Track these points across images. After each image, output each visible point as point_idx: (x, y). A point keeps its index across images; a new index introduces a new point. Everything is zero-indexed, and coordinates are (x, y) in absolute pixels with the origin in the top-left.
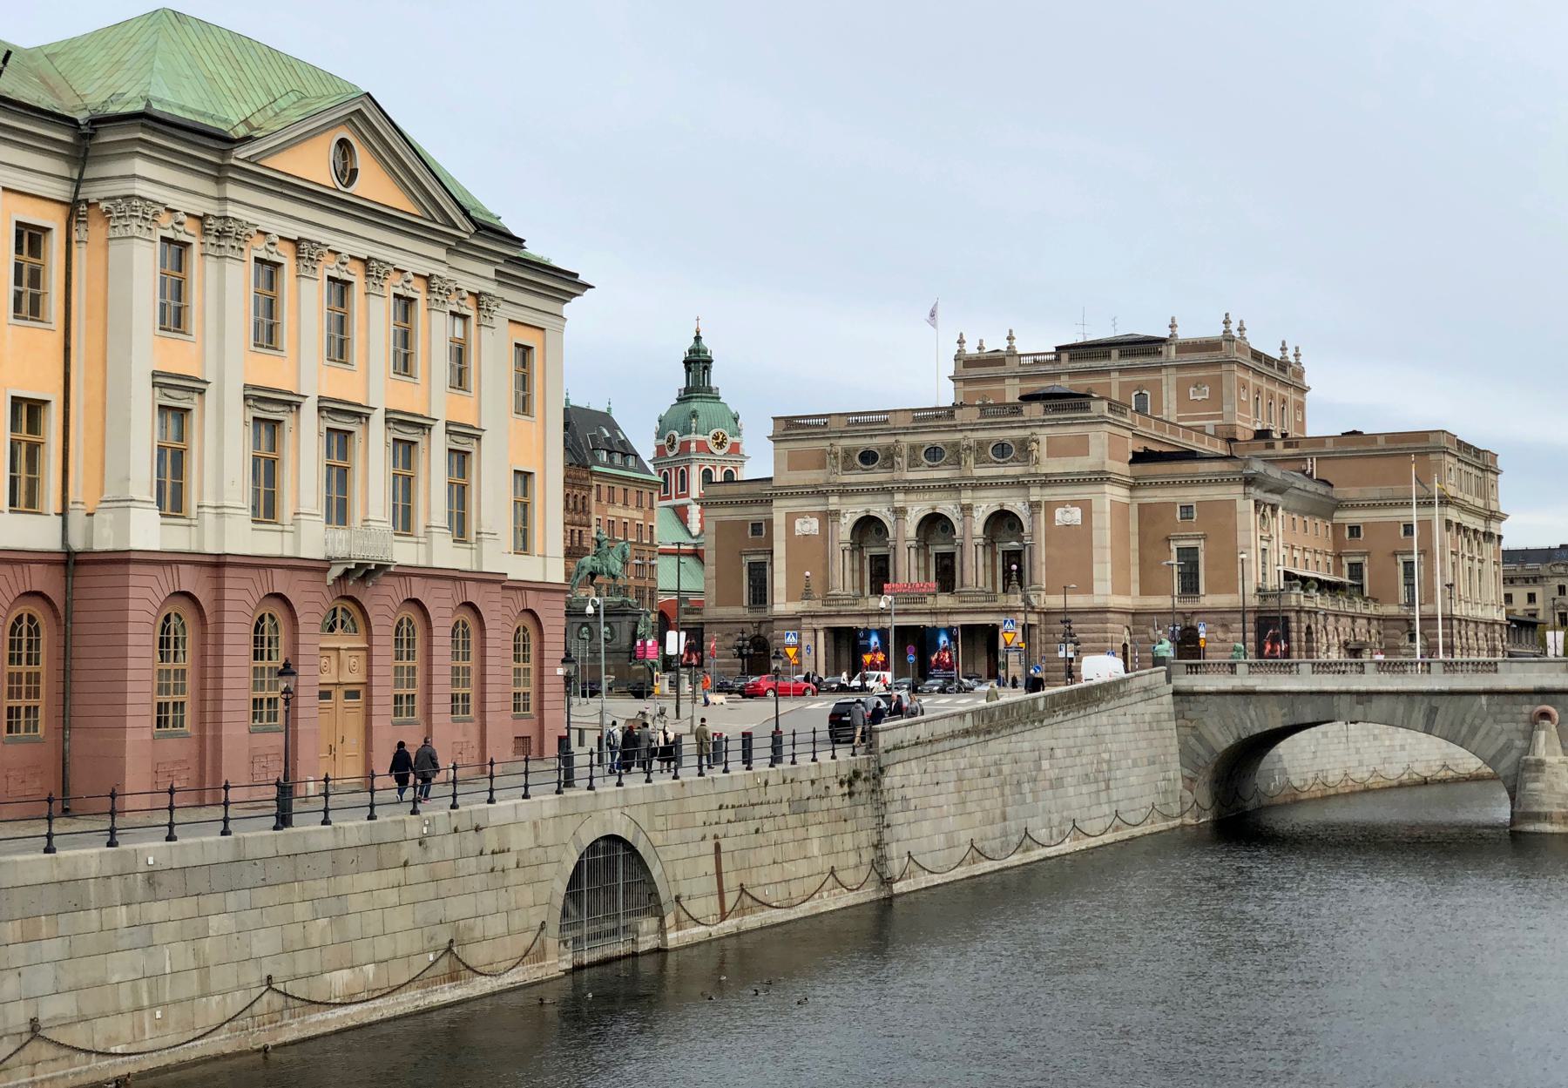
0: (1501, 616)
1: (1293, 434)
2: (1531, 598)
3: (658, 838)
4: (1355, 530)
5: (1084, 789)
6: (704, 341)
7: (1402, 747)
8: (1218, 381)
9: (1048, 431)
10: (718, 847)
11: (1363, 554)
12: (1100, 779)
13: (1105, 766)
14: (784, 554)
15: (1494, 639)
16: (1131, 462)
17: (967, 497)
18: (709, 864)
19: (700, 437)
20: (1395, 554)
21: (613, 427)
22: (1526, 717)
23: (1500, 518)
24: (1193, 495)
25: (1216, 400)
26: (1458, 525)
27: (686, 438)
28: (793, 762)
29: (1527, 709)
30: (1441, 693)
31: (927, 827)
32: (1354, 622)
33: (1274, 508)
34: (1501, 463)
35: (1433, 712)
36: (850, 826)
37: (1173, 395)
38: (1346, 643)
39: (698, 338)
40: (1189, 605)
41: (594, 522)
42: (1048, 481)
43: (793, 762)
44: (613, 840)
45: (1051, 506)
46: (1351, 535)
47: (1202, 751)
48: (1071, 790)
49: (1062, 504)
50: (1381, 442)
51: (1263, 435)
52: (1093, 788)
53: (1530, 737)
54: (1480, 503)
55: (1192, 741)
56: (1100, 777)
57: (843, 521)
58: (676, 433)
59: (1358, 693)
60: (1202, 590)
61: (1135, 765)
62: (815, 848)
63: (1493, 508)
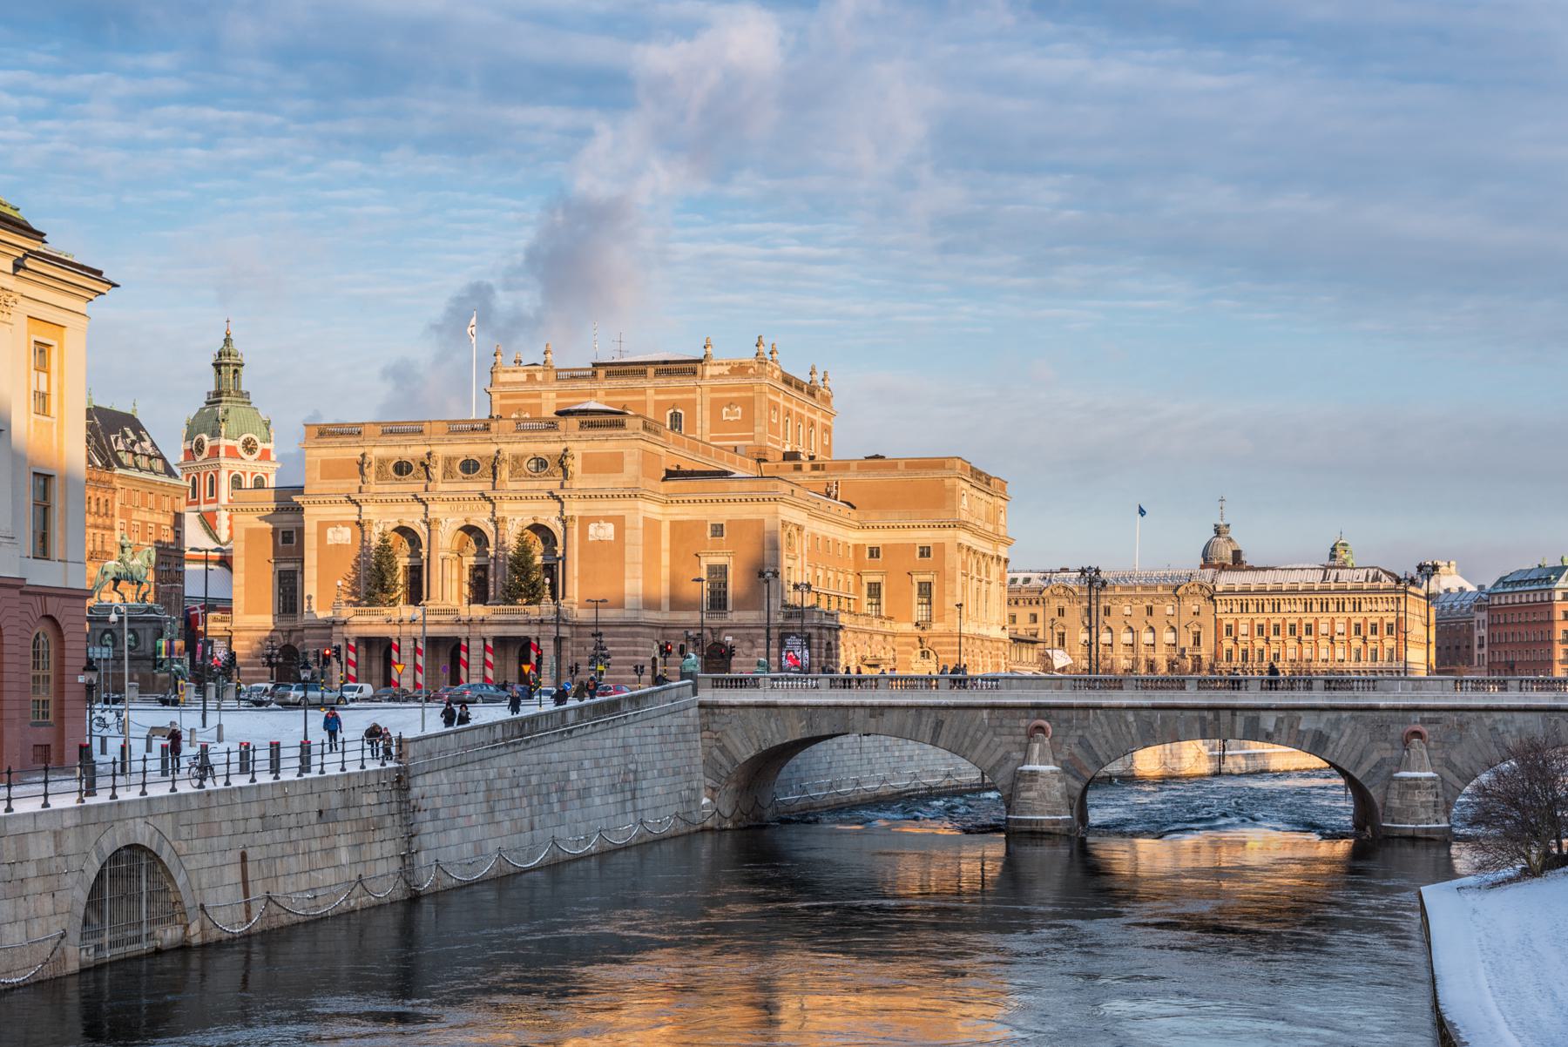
0: (1005, 636)
1: (819, 457)
2: (1034, 618)
3: (183, 847)
5: (611, 799)
6: (236, 346)
7: (911, 758)
9: (583, 445)
10: (244, 857)
12: (628, 787)
13: (631, 776)
16: (664, 480)
18: (233, 874)
19: (230, 442)
21: (137, 427)
22: (1023, 731)
26: (969, 549)
27: (214, 443)
28: (322, 772)
29: (1023, 723)
30: (947, 707)
31: (454, 836)
35: (939, 724)
36: (378, 835)
37: (707, 414)
39: (227, 341)
41: (117, 526)
43: (322, 772)
44: (135, 848)
45: (585, 521)
46: (871, 555)
47: (724, 762)
48: (597, 801)
51: (791, 456)
52: (620, 797)
53: (1026, 750)
54: (990, 528)
55: (716, 752)
56: (627, 787)
58: (205, 437)
59: (872, 707)
60: (730, 607)
61: (661, 775)
62: (344, 856)
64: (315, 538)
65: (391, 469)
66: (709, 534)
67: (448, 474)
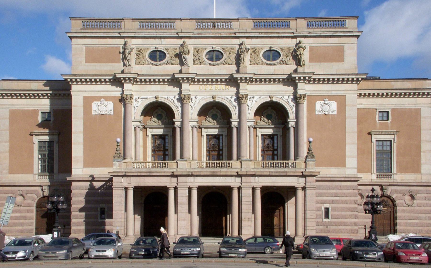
14: (81, 129)
17: (245, 88)
45: (313, 100)
57: (134, 103)
64: (82, 109)
65: (147, 56)
66: (377, 118)
67: (198, 61)
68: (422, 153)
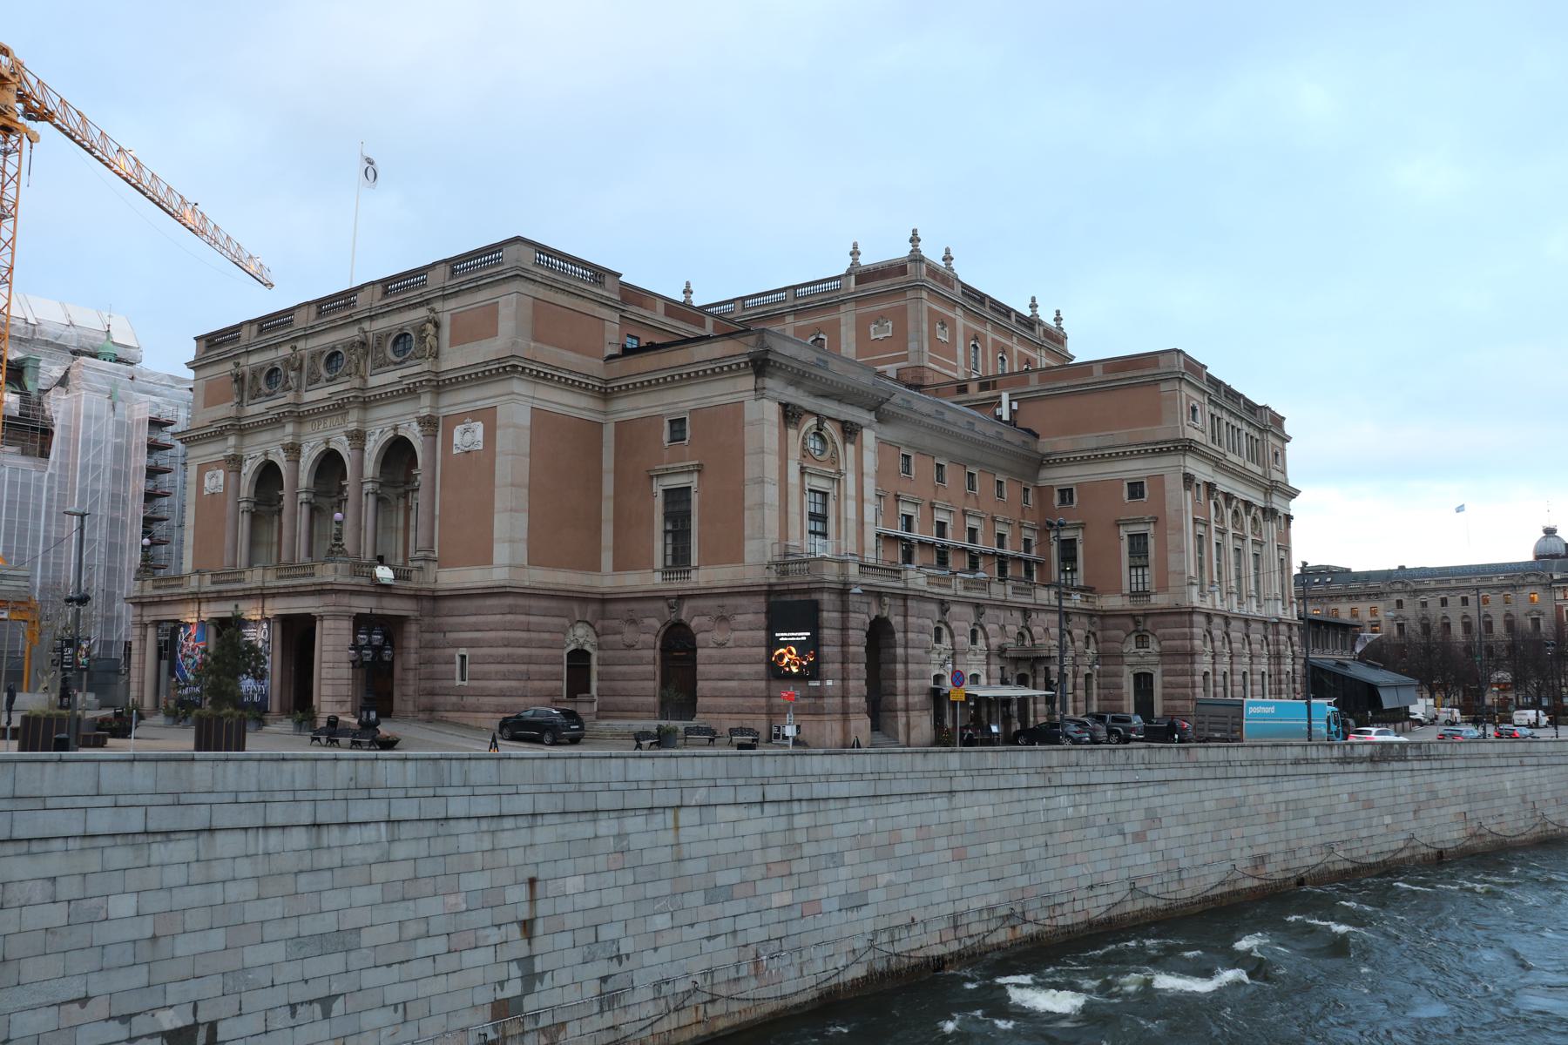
0: (1291, 614)
4: (1066, 494)
8: (900, 316)
9: (452, 304)
11: (1076, 527)
15: (1278, 643)
20: (1118, 524)
23: (1292, 494)
24: (684, 400)
25: (900, 337)
32: (980, 615)
33: (850, 431)
34: (1288, 428)
38: (1002, 650)
40: (677, 585)
42: (440, 385)
46: (1063, 501)
49: (460, 418)
50: (1098, 372)
57: (245, 470)
63: (1276, 476)
68: (747, 513)
